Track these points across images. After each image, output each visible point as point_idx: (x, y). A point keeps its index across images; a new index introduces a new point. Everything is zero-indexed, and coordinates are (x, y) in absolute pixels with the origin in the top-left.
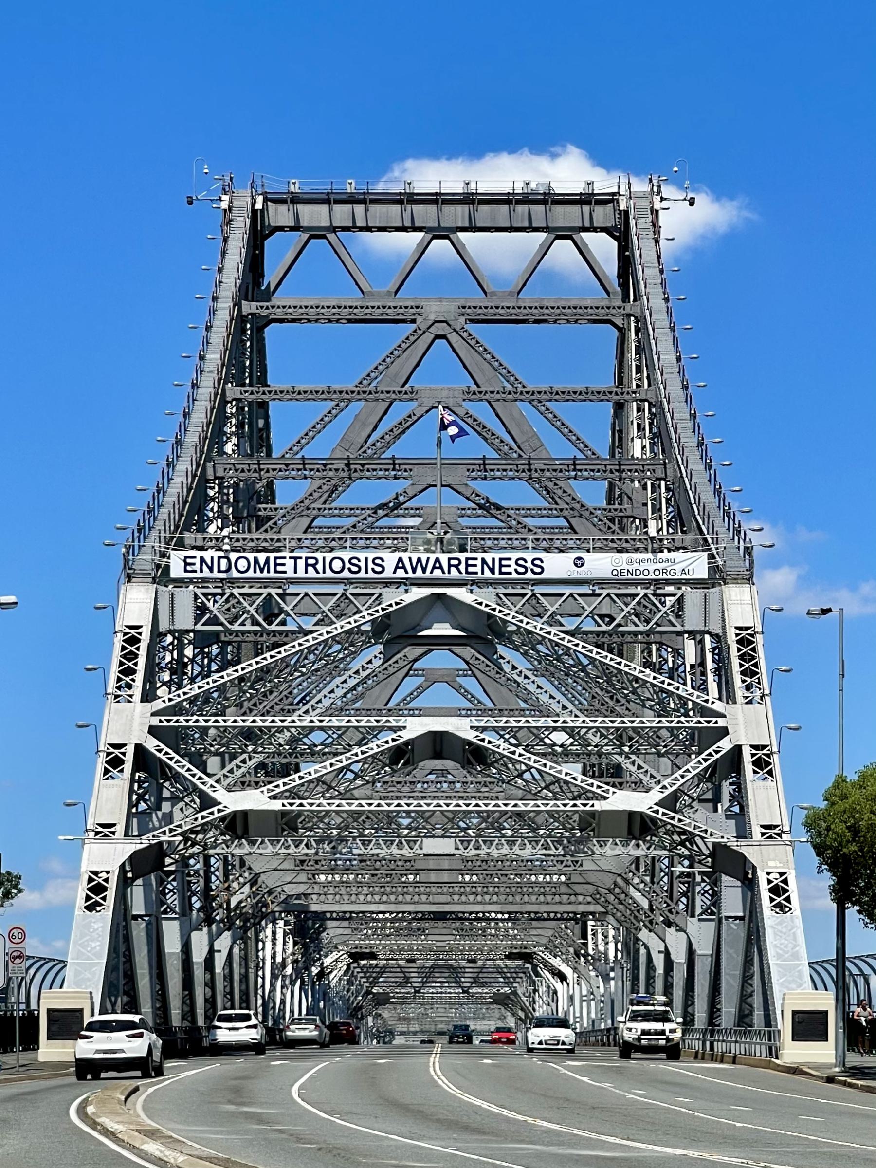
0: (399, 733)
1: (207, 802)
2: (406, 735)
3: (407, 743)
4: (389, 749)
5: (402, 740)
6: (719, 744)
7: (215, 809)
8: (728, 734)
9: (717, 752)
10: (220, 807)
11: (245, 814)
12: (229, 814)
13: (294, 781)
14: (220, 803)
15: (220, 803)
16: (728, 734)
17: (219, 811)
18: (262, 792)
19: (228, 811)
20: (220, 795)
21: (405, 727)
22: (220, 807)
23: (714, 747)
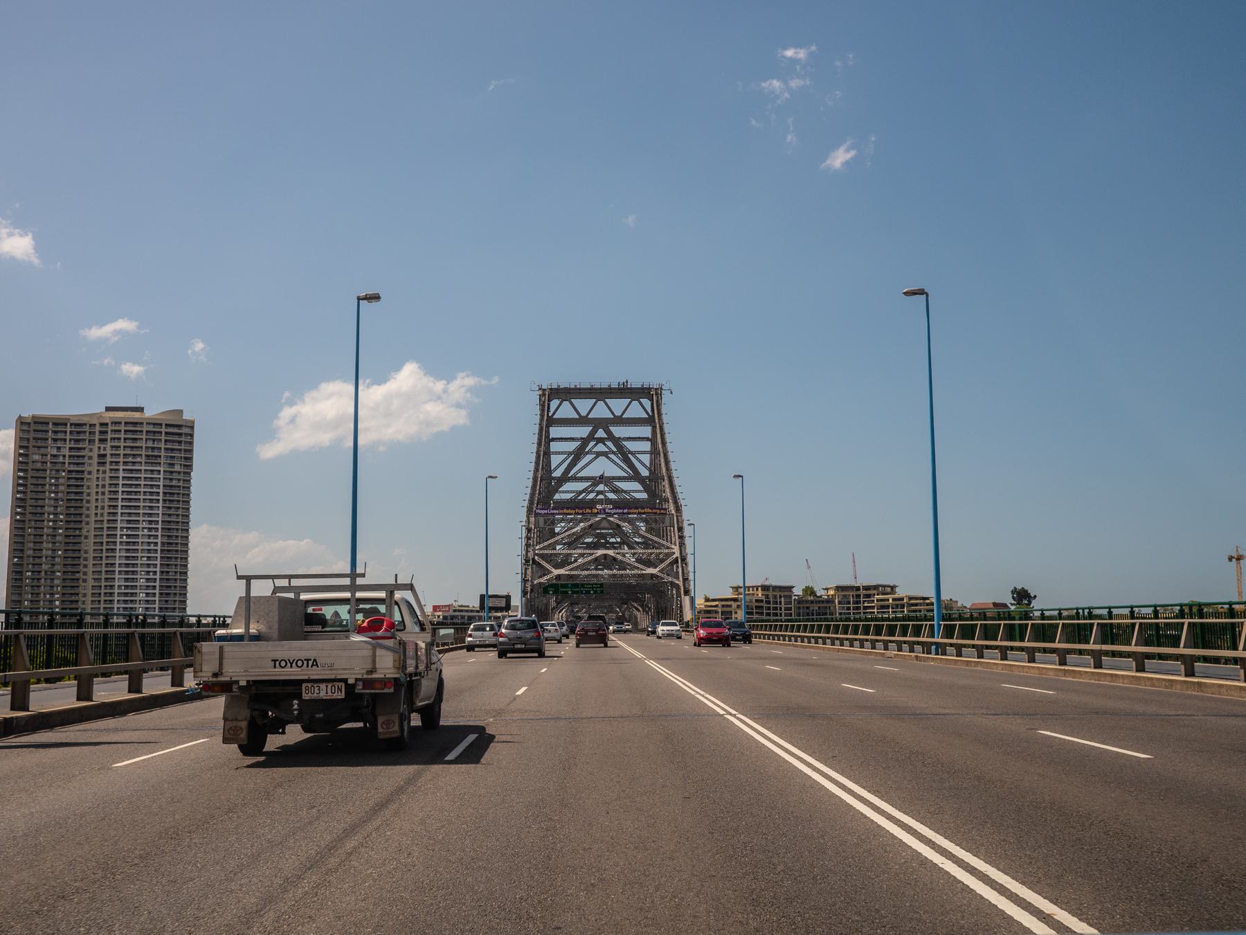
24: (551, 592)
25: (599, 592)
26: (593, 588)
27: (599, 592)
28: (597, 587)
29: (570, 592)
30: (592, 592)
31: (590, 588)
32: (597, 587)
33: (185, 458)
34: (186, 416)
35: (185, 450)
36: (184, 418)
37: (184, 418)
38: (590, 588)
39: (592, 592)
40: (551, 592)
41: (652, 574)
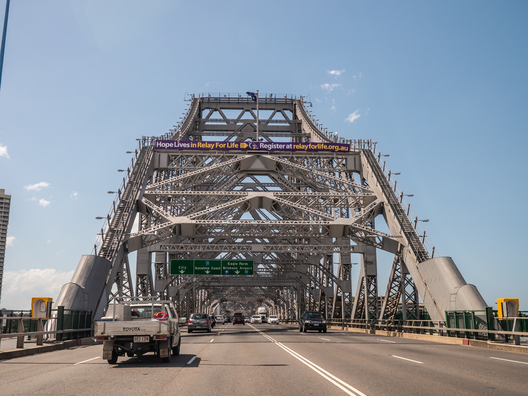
0: (246, 197)
1: (163, 220)
2: (248, 198)
3: (248, 201)
4: (241, 202)
5: (246, 199)
6: (374, 202)
7: (167, 223)
8: (377, 198)
9: (375, 204)
10: (169, 222)
11: (180, 225)
12: (173, 225)
13: (202, 213)
14: (169, 221)
15: (169, 221)
16: (377, 198)
17: (169, 224)
18: (188, 217)
19: (172, 224)
20: (170, 218)
21: (248, 195)
22: (169, 222)
23: (373, 203)
24: (182, 272)
25: (246, 272)
26: (238, 266)
27: (246, 272)
28: (244, 266)
29: (208, 272)
30: (237, 272)
31: (235, 266)
32: (244, 266)
33: (4, 217)
34: (6, 193)
35: (4, 212)
36: (5, 194)
37: (5, 194)
38: (235, 266)
39: (237, 272)
40: (182, 272)
41: (345, 227)
